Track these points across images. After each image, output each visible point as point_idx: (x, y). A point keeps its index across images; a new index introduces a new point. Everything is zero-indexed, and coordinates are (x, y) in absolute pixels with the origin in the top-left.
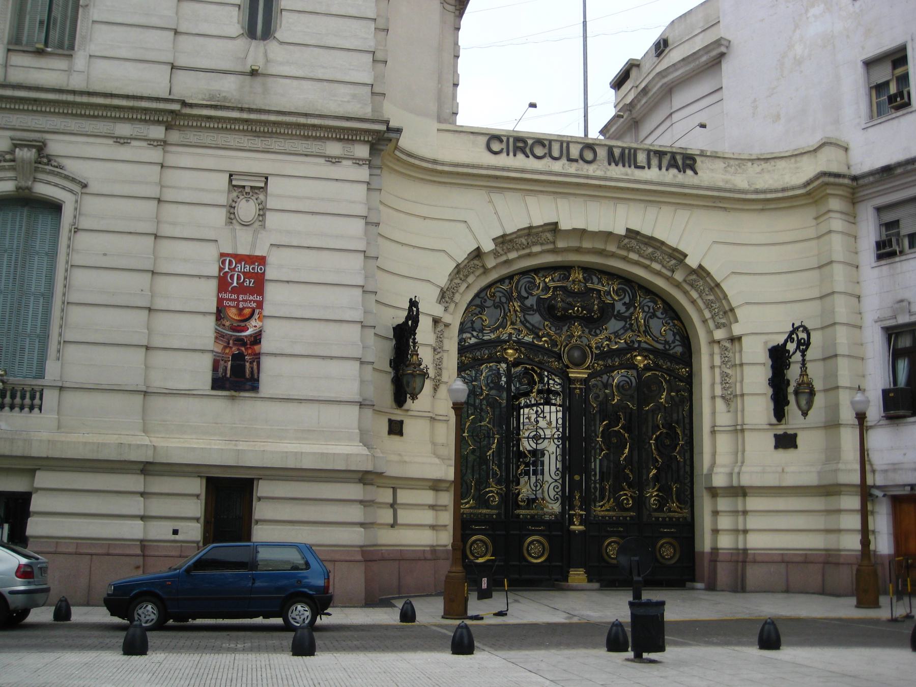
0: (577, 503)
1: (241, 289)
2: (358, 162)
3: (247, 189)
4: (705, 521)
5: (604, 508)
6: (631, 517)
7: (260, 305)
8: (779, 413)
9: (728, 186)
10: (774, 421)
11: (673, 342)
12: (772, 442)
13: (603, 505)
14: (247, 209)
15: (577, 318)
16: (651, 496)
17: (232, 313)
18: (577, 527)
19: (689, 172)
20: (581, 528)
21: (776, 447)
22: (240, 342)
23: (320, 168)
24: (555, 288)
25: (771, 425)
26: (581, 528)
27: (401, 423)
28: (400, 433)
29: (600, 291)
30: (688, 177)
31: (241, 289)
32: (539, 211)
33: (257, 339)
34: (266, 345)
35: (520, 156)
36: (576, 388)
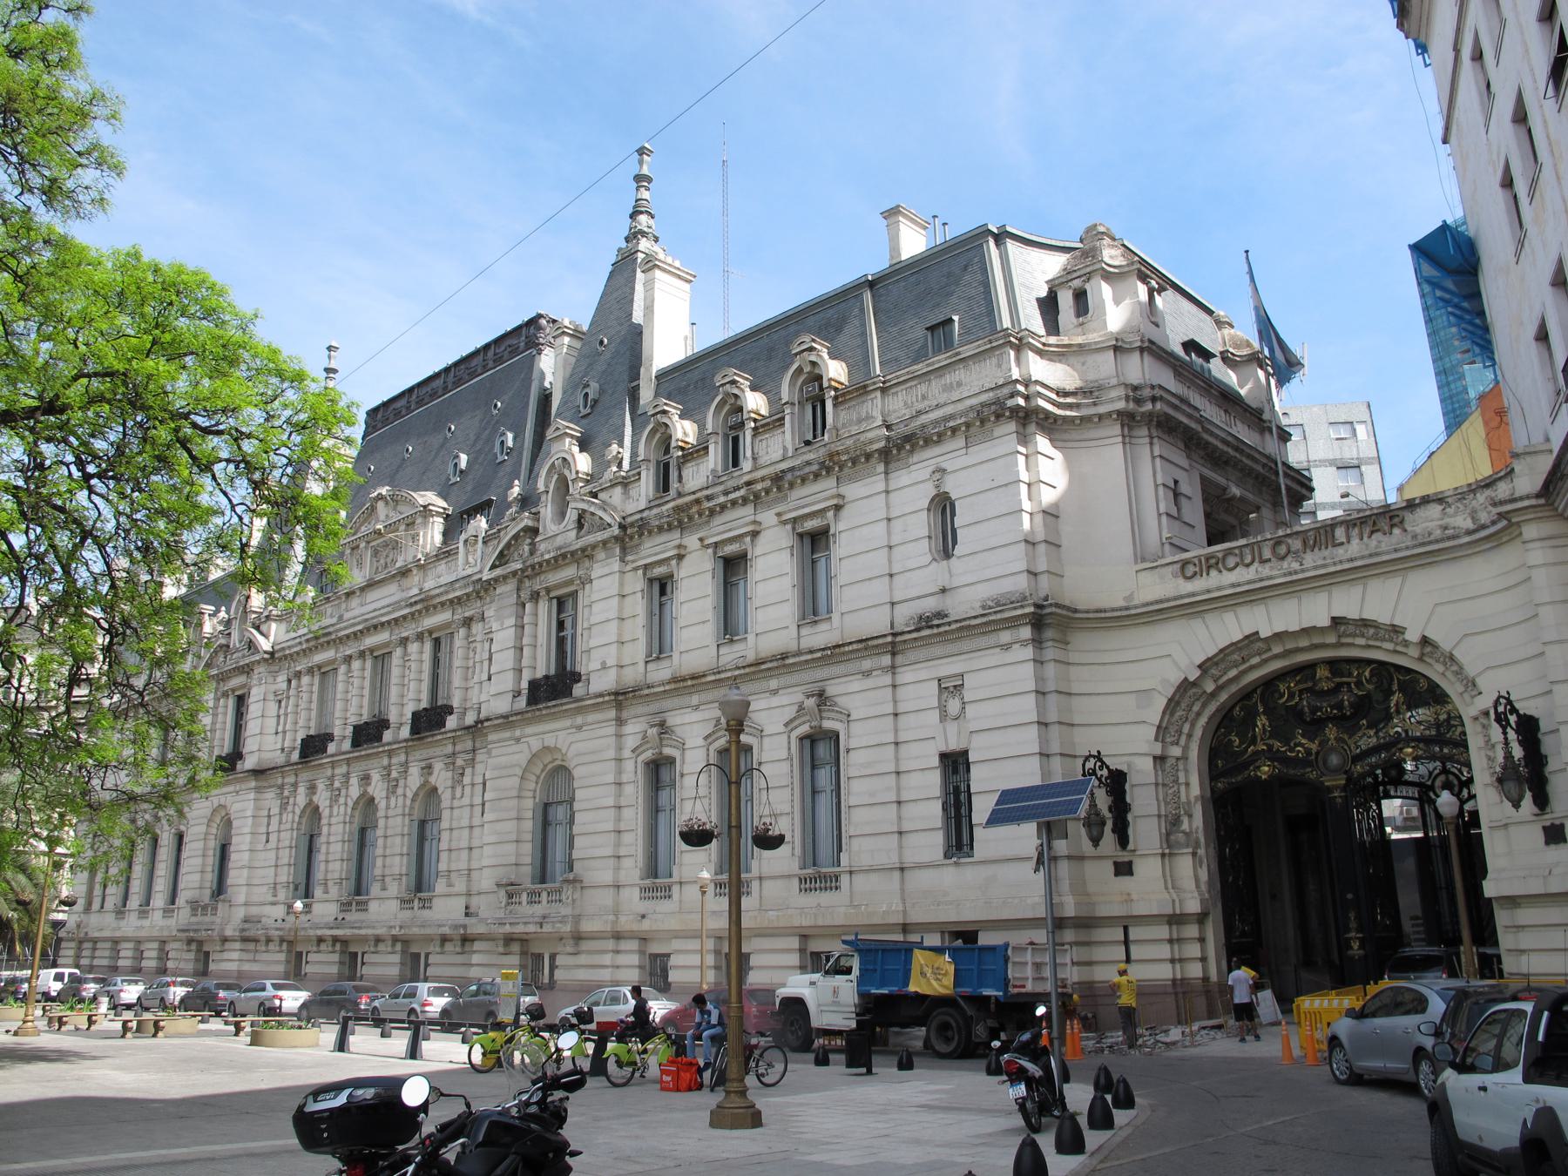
2: (1024, 643)
3: (951, 688)
10: (1536, 810)
14: (954, 706)
21: (1547, 843)
23: (995, 657)
24: (1301, 692)
27: (1130, 863)
28: (1131, 873)
32: (1230, 628)
35: (1213, 573)
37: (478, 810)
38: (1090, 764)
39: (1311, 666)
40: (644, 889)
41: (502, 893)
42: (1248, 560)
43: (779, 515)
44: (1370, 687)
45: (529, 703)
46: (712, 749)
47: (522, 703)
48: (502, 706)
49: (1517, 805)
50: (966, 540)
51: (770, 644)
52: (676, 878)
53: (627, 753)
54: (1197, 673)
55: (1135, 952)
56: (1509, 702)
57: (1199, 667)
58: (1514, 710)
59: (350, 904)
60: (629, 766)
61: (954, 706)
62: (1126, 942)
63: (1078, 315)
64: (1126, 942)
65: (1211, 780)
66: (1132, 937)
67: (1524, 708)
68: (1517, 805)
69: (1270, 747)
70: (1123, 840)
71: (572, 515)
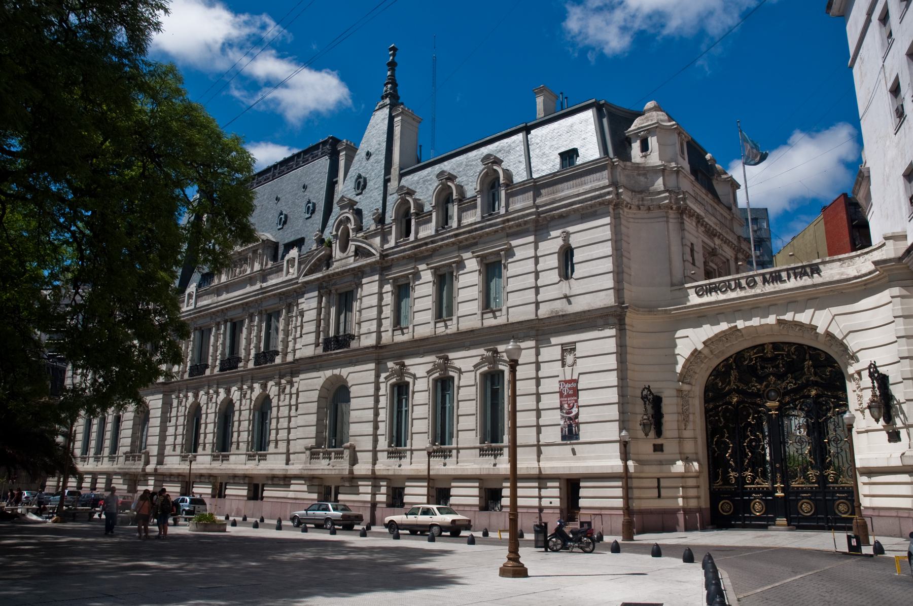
1: (568, 396)
3: (568, 349)
4: (863, 490)
7: (576, 401)
9: (844, 277)
14: (569, 359)
15: (772, 374)
17: (566, 406)
18: (779, 494)
19: (815, 275)
21: (890, 441)
22: (570, 419)
30: (817, 279)
31: (568, 396)
33: (577, 416)
34: (581, 419)
35: (713, 294)
37: (294, 408)
38: (645, 393)
39: (763, 345)
40: (389, 453)
41: (308, 452)
42: (733, 287)
43: (473, 253)
45: (325, 350)
46: (431, 378)
47: (320, 350)
48: (309, 352)
49: (877, 420)
50: (579, 271)
51: (467, 324)
52: (408, 447)
53: (382, 379)
54: (703, 346)
55: (664, 492)
56: (875, 367)
57: (704, 343)
58: (877, 372)
59: (218, 456)
60: (383, 386)
61: (569, 359)
62: (659, 487)
63: (642, 151)
64: (659, 487)
65: (705, 402)
66: (662, 485)
67: (882, 370)
68: (877, 420)
69: (738, 387)
70: (659, 433)
71: (352, 248)
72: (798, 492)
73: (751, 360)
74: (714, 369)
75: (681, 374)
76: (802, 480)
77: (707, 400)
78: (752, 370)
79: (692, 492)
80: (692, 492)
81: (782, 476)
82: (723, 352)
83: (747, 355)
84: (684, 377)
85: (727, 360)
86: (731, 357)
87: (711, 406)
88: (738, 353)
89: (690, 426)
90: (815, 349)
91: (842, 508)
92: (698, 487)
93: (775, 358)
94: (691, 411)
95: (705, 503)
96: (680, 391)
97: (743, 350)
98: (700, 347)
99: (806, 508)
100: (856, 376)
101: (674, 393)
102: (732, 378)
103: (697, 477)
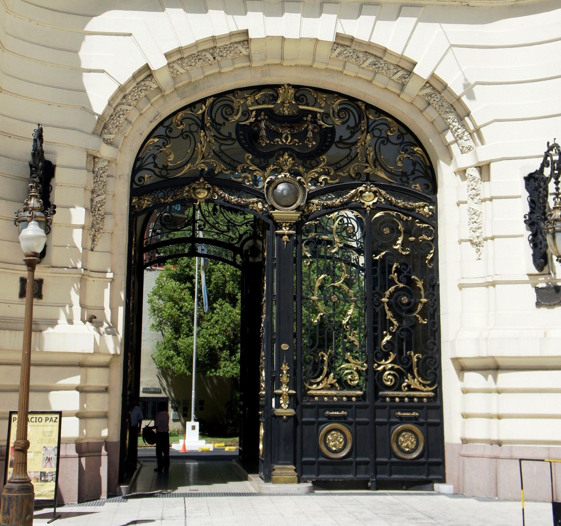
0: (285, 379)
5: (321, 386)
6: (357, 397)
8: (541, 259)
10: (535, 271)
11: (413, 173)
12: (533, 296)
13: (321, 382)
15: (285, 149)
16: (384, 370)
20: (291, 412)
24: (259, 111)
25: (529, 275)
26: (291, 412)
29: (316, 113)
36: (284, 235)
39: (275, 87)
44: (338, 121)
69: (212, 170)
72: (322, 406)
73: (246, 113)
74: (161, 124)
75: (101, 118)
76: (331, 379)
77: (137, 190)
78: (248, 136)
79: (97, 404)
80: (97, 404)
81: (293, 373)
82: (193, 85)
83: (238, 102)
84: (103, 127)
85: (192, 106)
86: (203, 101)
87: (146, 202)
88: (218, 96)
89: (102, 243)
90: (379, 111)
91: (407, 442)
92: (106, 390)
93: (296, 120)
94: (108, 207)
95: (108, 431)
96: (93, 158)
97: (232, 92)
98: (158, 63)
99: (336, 442)
100: (475, 173)
101: (82, 160)
102: (202, 148)
103: (106, 366)
